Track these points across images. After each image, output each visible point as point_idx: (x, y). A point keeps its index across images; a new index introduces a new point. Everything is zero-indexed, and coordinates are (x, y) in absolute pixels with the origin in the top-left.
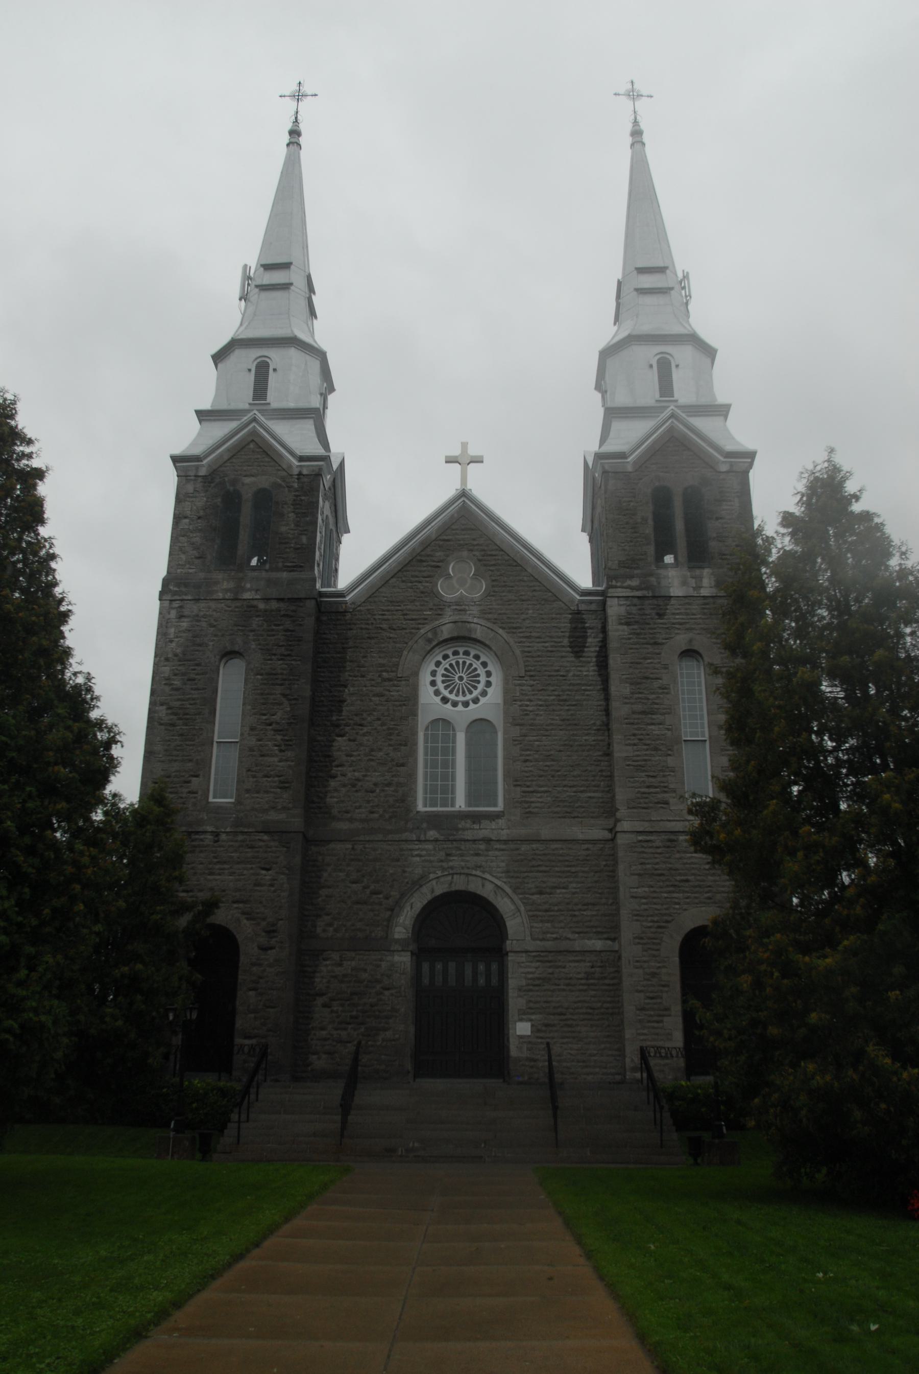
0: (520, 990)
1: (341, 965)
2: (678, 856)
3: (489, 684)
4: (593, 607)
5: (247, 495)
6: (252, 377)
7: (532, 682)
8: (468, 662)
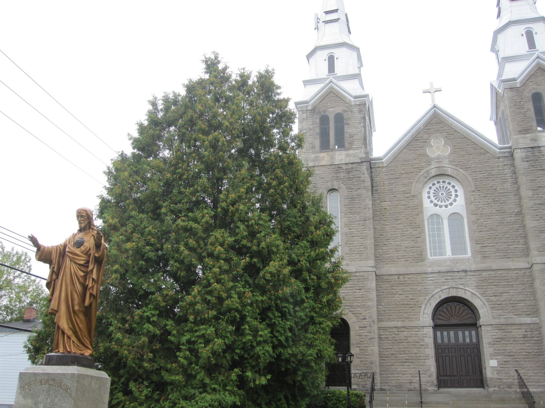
0: (489, 344)
1: (398, 334)
3: (456, 196)
4: (506, 155)
5: (332, 117)
6: (327, 63)
7: (479, 194)
8: (445, 186)
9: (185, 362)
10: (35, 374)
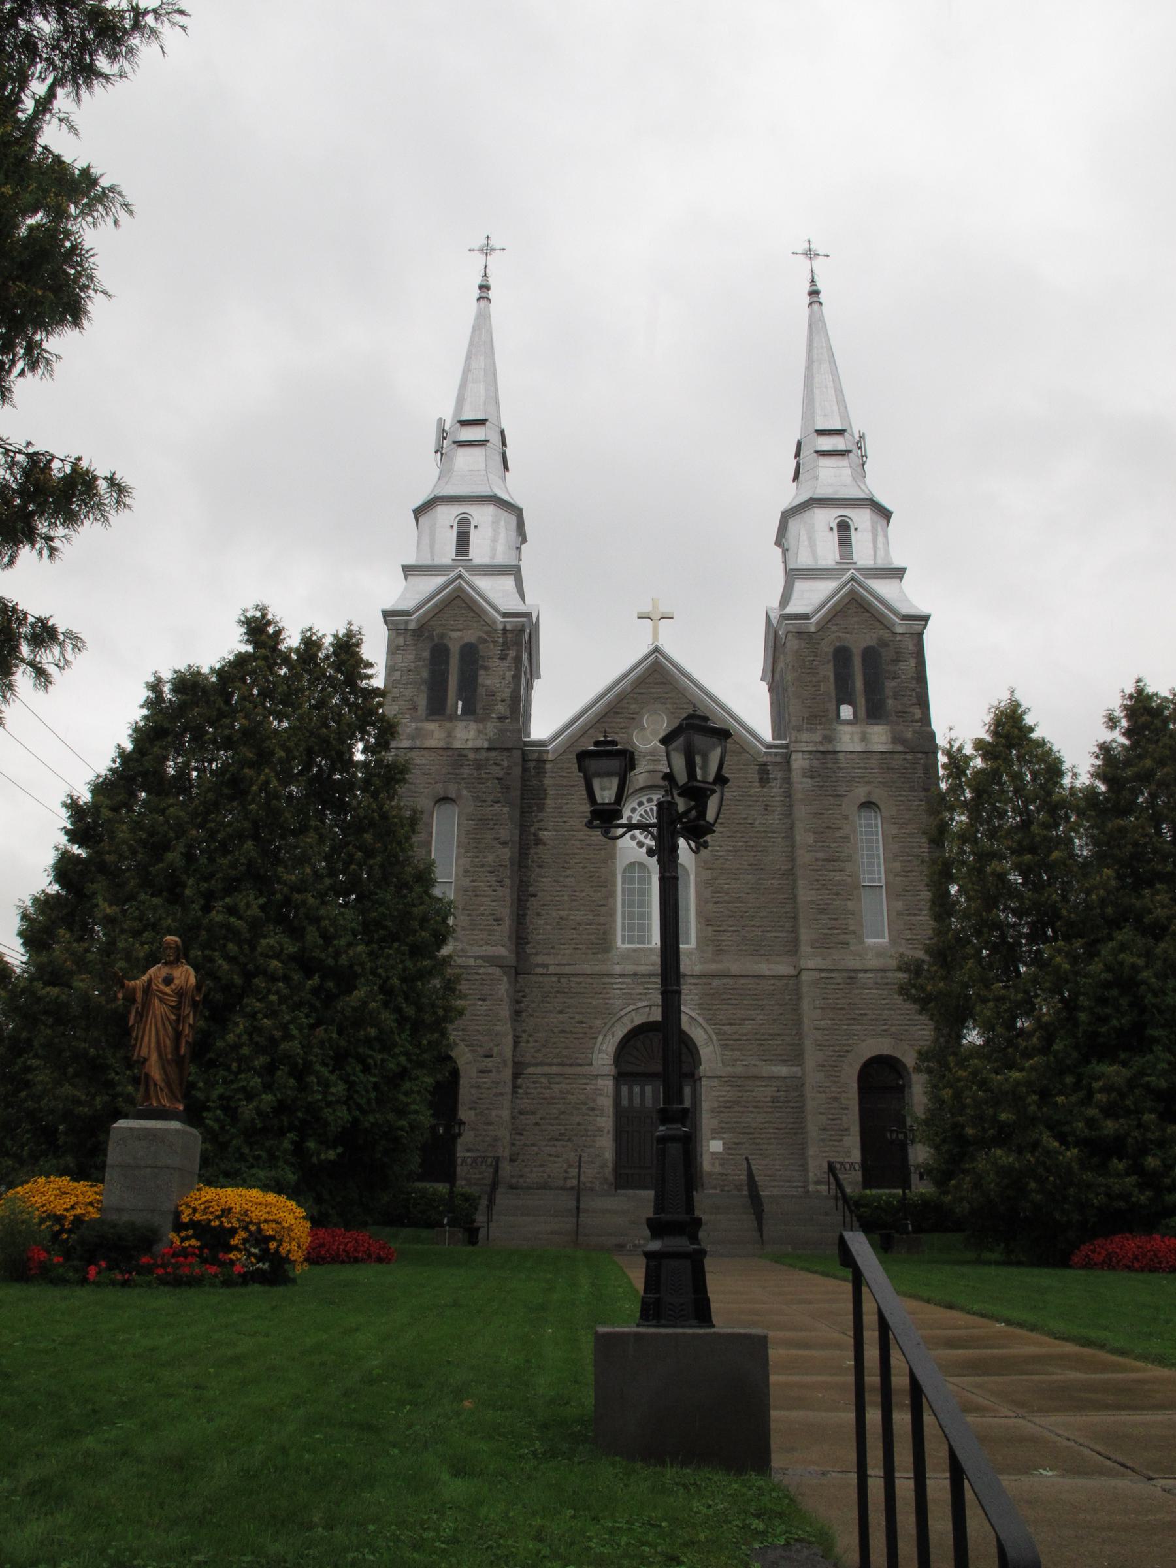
1: (549, 1088)
2: (857, 992)
4: (778, 759)
6: (454, 533)
9: (216, 1127)
10: (131, 1129)
